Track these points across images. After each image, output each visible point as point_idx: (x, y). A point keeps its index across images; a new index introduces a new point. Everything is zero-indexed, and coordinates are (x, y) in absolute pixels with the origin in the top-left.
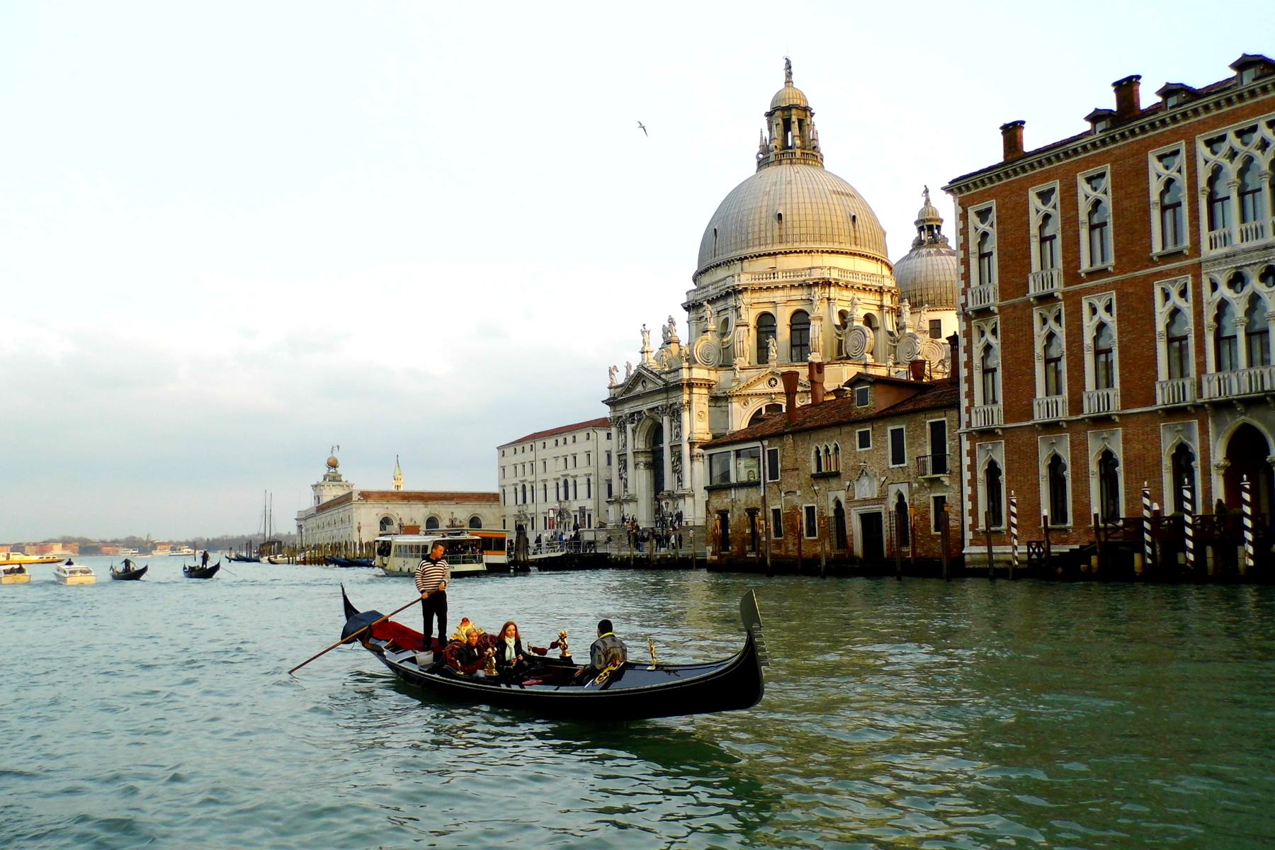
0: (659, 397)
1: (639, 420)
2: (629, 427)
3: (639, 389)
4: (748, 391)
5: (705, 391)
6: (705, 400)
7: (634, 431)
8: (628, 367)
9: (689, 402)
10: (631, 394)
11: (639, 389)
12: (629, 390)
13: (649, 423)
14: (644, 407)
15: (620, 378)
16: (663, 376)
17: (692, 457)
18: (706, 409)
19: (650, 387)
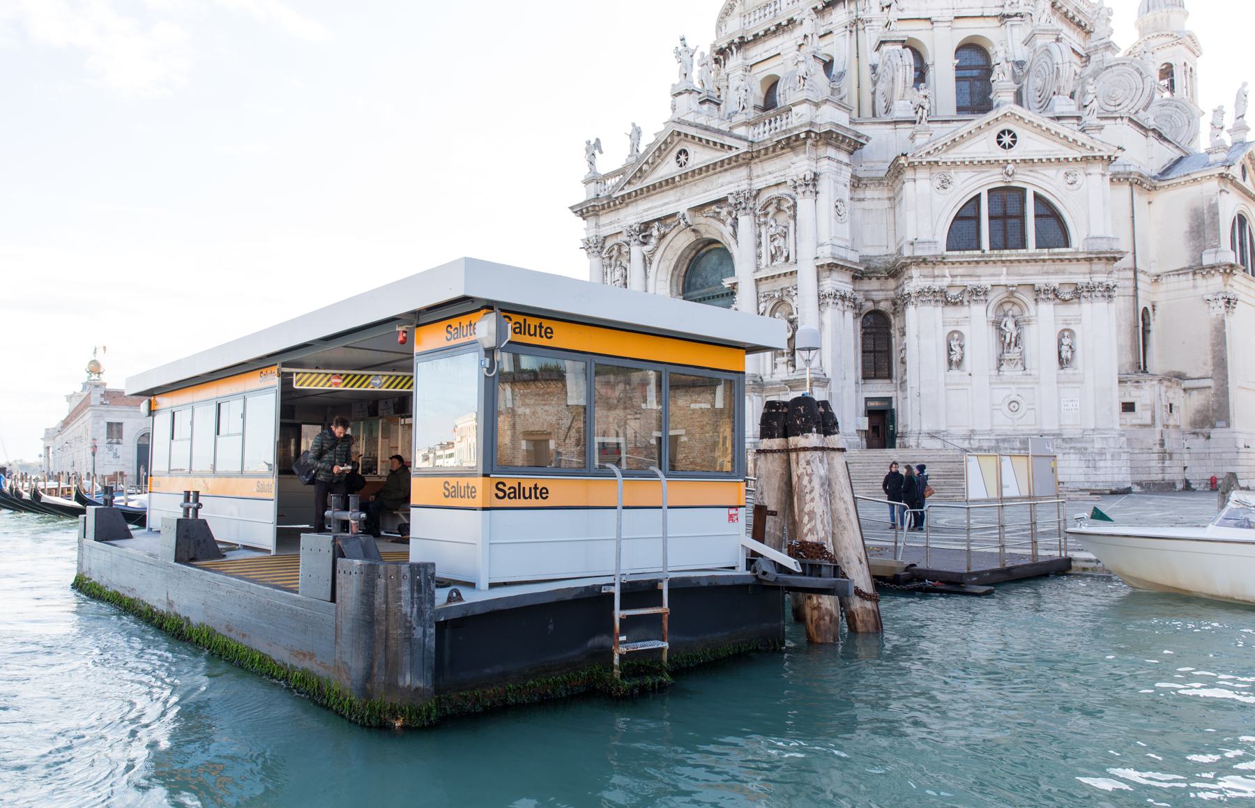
0: (727, 177)
1: (663, 236)
2: (637, 251)
3: (669, 168)
4: (951, 156)
5: (844, 157)
6: (847, 173)
7: (647, 261)
8: (637, 133)
9: (816, 177)
10: (649, 181)
11: (669, 168)
12: (640, 174)
13: (682, 241)
14: (679, 202)
15: (614, 158)
16: (741, 131)
17: (822, 298)
18: (846, 194)
19: (699, 157)
